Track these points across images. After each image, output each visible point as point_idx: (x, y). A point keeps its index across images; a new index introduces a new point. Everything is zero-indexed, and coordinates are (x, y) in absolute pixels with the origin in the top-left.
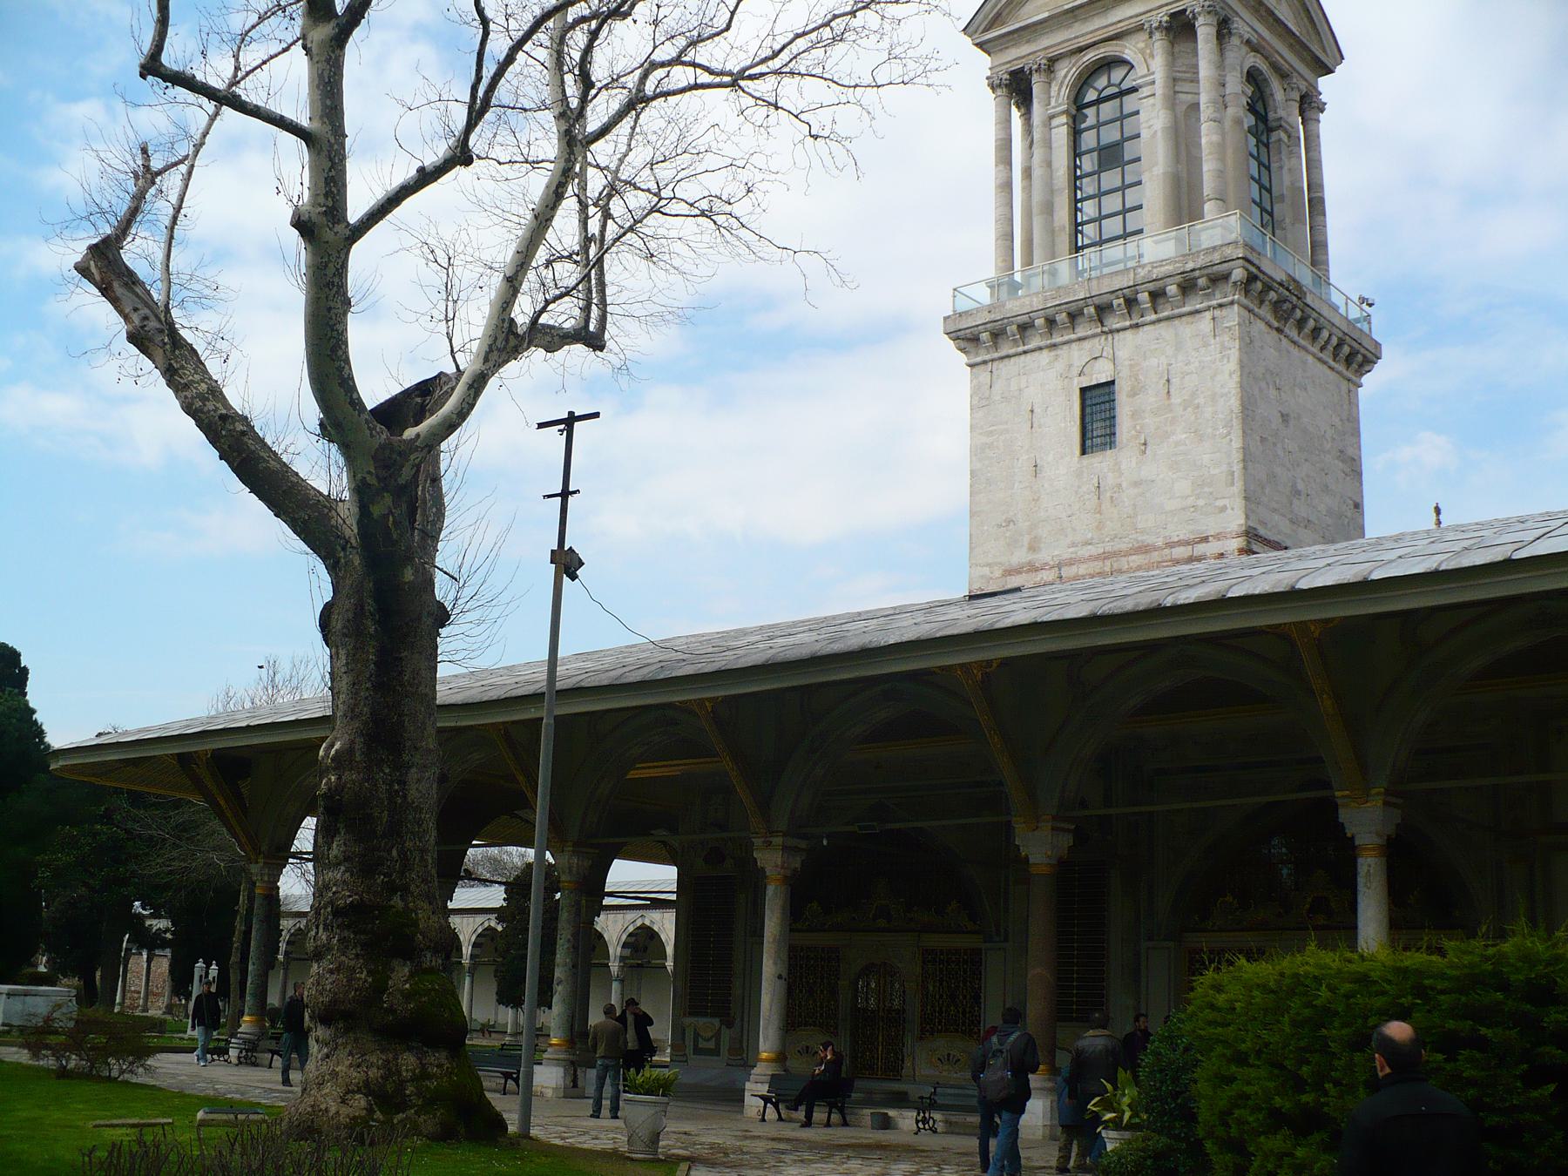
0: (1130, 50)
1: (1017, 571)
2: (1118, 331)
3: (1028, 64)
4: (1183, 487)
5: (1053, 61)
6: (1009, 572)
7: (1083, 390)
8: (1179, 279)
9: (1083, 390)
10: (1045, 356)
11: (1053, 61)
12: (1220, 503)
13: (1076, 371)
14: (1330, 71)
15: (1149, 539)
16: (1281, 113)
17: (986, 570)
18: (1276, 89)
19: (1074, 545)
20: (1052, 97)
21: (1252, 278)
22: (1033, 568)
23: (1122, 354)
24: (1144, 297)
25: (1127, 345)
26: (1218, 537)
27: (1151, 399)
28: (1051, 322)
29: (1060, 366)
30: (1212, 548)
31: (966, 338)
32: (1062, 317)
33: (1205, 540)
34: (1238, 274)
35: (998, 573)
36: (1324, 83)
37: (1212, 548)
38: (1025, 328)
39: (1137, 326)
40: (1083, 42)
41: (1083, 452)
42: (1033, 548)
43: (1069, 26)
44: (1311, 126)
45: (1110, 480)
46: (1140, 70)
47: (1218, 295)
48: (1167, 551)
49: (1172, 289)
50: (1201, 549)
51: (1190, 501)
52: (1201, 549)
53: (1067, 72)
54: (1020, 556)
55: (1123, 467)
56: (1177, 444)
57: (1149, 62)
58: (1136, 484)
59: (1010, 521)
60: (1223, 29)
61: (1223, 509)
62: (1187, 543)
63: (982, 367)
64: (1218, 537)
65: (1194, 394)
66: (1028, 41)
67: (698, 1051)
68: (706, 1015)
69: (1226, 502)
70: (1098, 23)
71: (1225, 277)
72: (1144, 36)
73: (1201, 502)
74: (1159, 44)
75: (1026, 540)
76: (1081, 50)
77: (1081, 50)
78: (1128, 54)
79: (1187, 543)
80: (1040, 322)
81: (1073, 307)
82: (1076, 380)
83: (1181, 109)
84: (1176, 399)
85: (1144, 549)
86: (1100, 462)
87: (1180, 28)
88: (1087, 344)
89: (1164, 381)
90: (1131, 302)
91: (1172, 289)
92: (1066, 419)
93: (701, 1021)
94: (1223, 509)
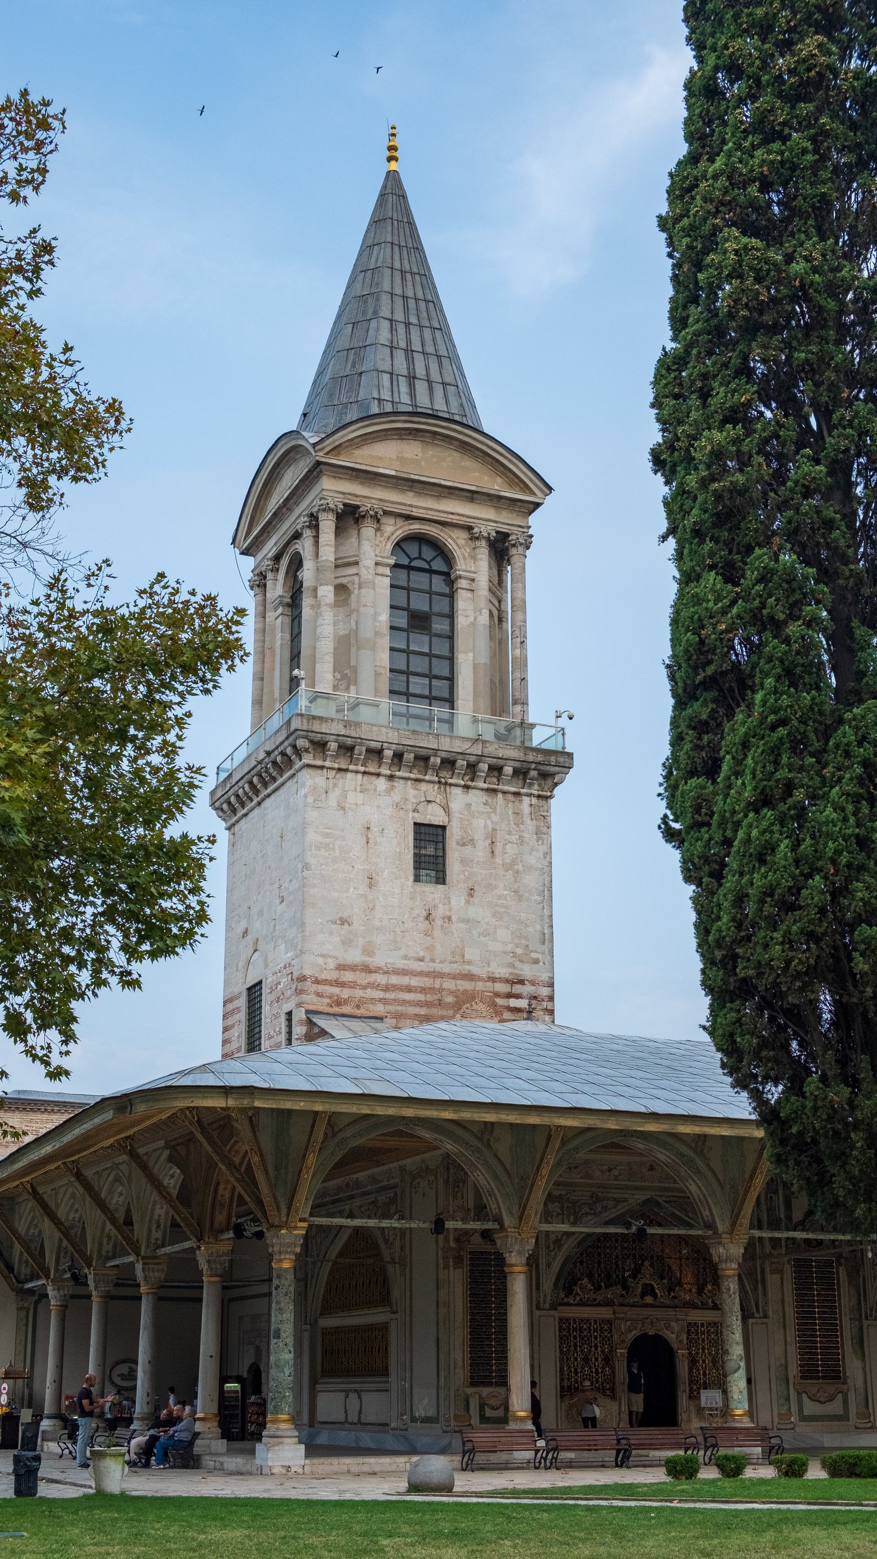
0: (455, 542)
1: (353, 968)
2: (451, 785)
3: (366, 506)
4: (503, 934)
6: (341, 967)
8: (517, 764)
10: (382, 784)
12: (534, 955)
13: (410, 807)
15: (475, 970)
17: (320, 961)
19: (406, 957)
22: (367, 969)
25: (458, 799)
26: (533, 983)
27: (480, 852)
28: (398, 756)
29: (396, 796)
30: (527, 989)
32: (409, 757)
33: (521, 982)
35: (332, 964)
37: (527, 989)
39: (467, 787)
40: (416, 513)
42: (368, 951)
43: (403, 491)
45: (441, 911)
47: (536, 787)
48: (490, 984)
49: (508, 770)
50: (517, 989)
51: (510, 947)
52: (517, 989)
53: (394, 530)
54: (354, 956)
55: (453, 902)
56: (500, 897)
58: (467, 921)
59: (343, 921)
61: (536, 962)
62: (507, 981)
63: (319, 771)
64: (533, 983)
65: (514, 862)
66: (362, 483)
67: (484, 1419)
68: (490, 1384)
69: (540, 956)
70: (430, 503)
73: (519, 951)
74: (483, 553)
75: (361, 942)
77: (408, 518)
78: (451, 544)
79: (507, 981)
80: (388, 753)
82: (411, 814)
84: (498, 860)
85: (470, 977)
86: (432, 892)
88: (424, 786)
89: (489, 841)
90: (472, 767)
91: (508, 770)
92: (399, 847)
93: (486, 1391)
94: (536, 962)
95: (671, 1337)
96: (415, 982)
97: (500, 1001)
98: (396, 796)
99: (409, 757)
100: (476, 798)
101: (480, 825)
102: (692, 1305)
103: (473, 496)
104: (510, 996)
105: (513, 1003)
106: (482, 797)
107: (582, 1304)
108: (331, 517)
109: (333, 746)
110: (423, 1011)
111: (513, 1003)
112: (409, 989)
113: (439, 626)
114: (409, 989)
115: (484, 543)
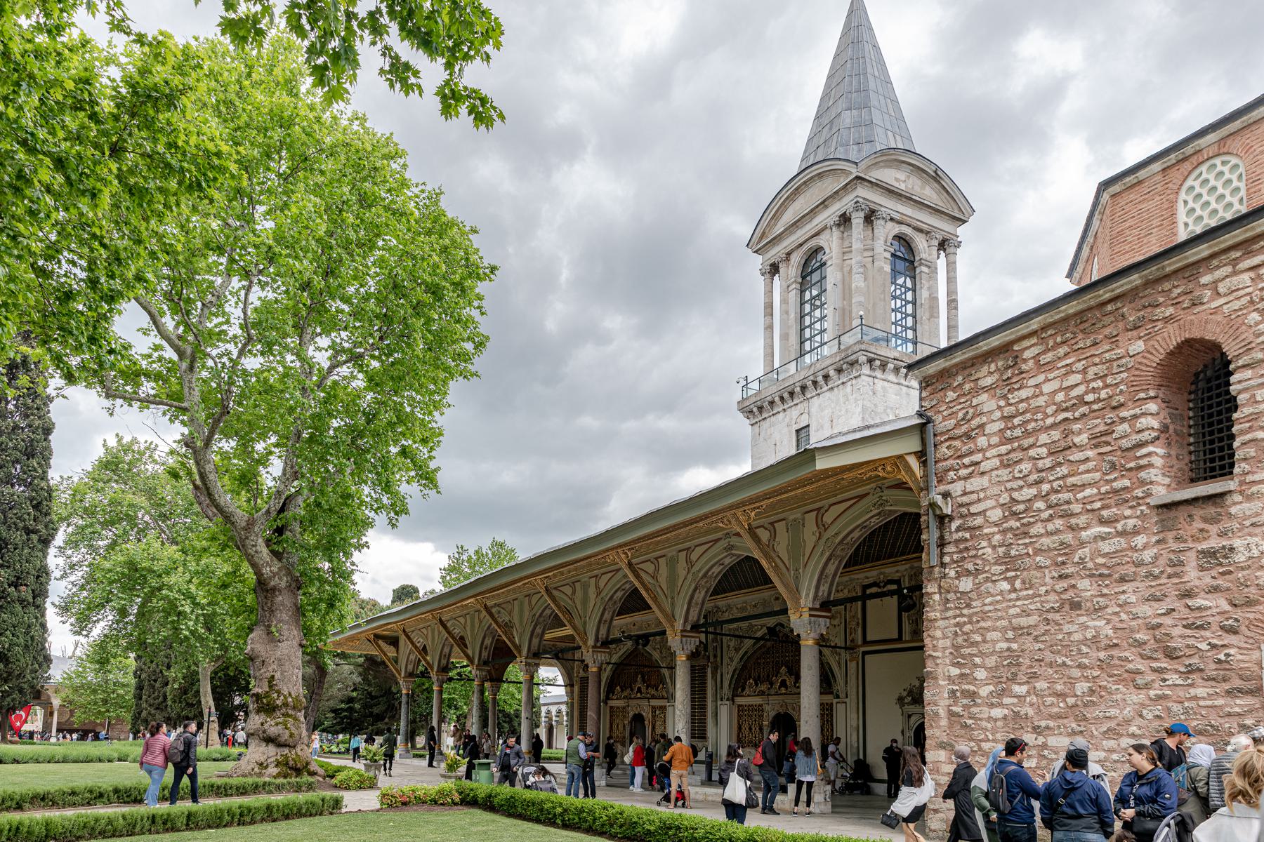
0: (822, 241)
5: (789, 254)
7: (798, 431)
9: (798, 431)
11: (789, 254)
14: (965, 222)
16: (923, 256)
18: (920, 242)
20: (791, 271)
21: (870, 361)
23: (813, 410)
24: (820, 379)
28: (782, 398)
29: (787, 420)
31: (748, 413)
32: (786, 395)
34: (863, 359)
36: (962, 232)
38: (772, 403)
40: (801, 240)
44: (951, 258)
46: (827, 251)
49: (832, 373)
53: (797, 258)
60: (870, 218)
70: (808, 227)
71: (857, 361)
72: (828, 231)
76: (801, 245)
77: (801, 245)
78: (822, 243)
80: (777, 399)
81: (790, 389)
83: (846, 269)
87: (845, 220)
90: (815, 383)
91: (832, 373)
98: (787, 420)
99: (786, 395)
101: (827, 412)
103: (824, 204)
106: (828, 394)
109: (755, 410)
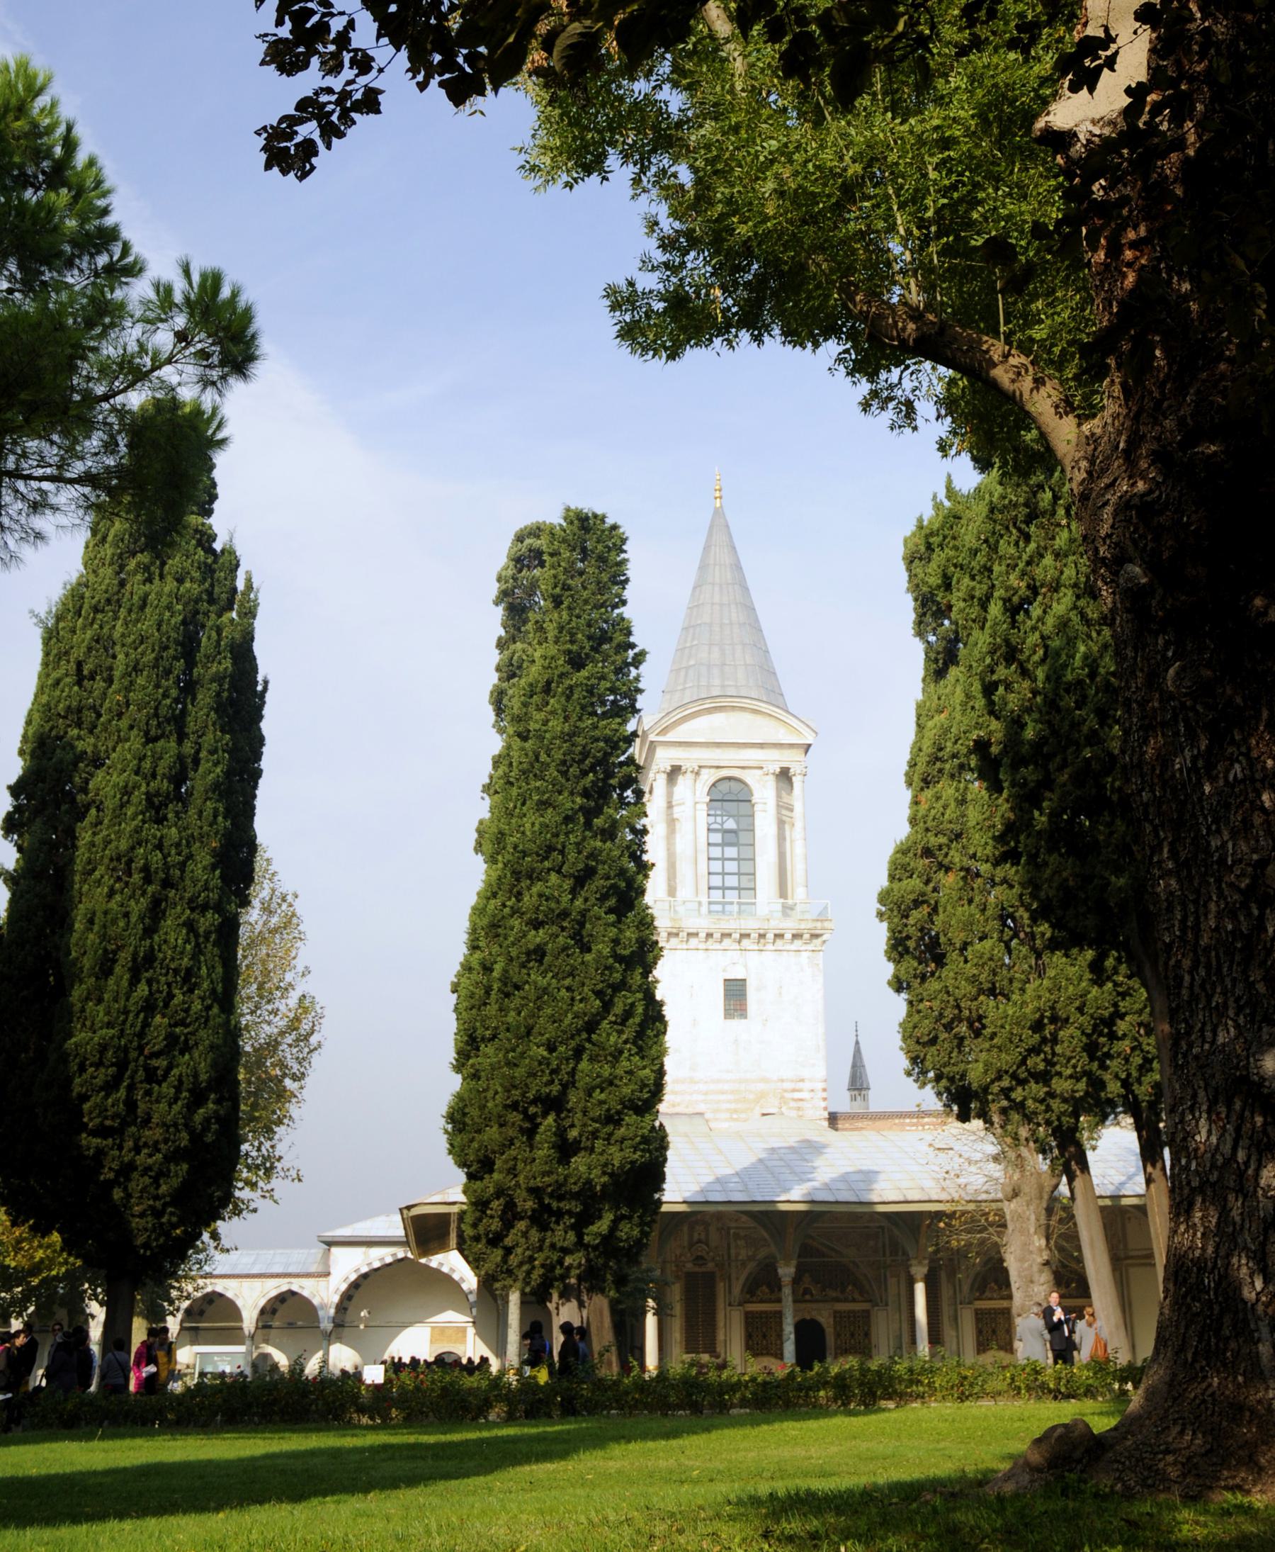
0: (749, 777)
3: (686, 765)
10: (701, 954)
25: (754, 959)
28: (709, 935)
30: (807, 1085)
41: (729, 1014)
50: (800, 1085)
52: (800, 1085)
53: (708, 777)
57: (764, 793)
72: (759, 772)
74: (771, 781)
78: (748, 780)
85: (765, 1080)
86: (736, 1024)
90: (762, 936)
95: (822, 1320)
96: (726, 1087)
97: (788, 1095)
100: (768, 957)
102: (837, 1300)
104: (794, 1090)
105: (797, 1095)
107: (762, 1301)
108: (664, 776)
110: (733, 1106)
111: (797, 1095)
112: (723, 1093)
113: (744, 838)
114: (723, 1093)
115: (772, 779)
